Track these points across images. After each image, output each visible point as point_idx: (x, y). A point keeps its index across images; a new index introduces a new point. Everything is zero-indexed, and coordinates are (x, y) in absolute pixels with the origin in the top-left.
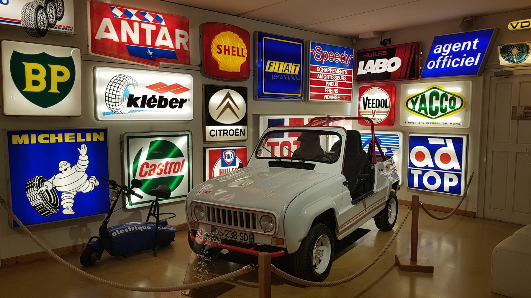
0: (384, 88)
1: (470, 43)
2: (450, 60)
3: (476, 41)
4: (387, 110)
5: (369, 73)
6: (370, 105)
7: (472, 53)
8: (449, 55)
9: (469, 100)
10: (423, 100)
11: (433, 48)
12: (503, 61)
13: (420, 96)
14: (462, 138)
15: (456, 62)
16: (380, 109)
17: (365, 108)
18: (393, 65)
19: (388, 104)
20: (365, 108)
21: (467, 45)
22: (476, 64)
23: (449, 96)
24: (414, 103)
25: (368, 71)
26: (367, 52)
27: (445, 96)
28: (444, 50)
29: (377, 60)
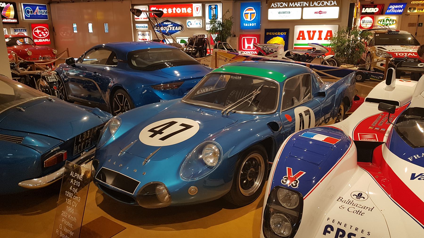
0: (371, 17)
1: (400, 6)
2: (394, 10)
3: (402, 6)
4: (372, 24)
5: (366, 12)
6: (365, 22)
7: (401, 9)
8: (394, 9)
9: (397, 21)
11: (389, 6)
12: (408, 11)
13: (383, 20)
15: (396, 11)
16: (369, 23)
18: (376, 10)
19: (372, 22)
21: (399, 6)
22: (401, 12)
23: (392, 20)
24: (381, 22)
25: (366, 11)
26: (367, 5)
27: (391, 20)
28: (392, 7)
29: (370, 8)
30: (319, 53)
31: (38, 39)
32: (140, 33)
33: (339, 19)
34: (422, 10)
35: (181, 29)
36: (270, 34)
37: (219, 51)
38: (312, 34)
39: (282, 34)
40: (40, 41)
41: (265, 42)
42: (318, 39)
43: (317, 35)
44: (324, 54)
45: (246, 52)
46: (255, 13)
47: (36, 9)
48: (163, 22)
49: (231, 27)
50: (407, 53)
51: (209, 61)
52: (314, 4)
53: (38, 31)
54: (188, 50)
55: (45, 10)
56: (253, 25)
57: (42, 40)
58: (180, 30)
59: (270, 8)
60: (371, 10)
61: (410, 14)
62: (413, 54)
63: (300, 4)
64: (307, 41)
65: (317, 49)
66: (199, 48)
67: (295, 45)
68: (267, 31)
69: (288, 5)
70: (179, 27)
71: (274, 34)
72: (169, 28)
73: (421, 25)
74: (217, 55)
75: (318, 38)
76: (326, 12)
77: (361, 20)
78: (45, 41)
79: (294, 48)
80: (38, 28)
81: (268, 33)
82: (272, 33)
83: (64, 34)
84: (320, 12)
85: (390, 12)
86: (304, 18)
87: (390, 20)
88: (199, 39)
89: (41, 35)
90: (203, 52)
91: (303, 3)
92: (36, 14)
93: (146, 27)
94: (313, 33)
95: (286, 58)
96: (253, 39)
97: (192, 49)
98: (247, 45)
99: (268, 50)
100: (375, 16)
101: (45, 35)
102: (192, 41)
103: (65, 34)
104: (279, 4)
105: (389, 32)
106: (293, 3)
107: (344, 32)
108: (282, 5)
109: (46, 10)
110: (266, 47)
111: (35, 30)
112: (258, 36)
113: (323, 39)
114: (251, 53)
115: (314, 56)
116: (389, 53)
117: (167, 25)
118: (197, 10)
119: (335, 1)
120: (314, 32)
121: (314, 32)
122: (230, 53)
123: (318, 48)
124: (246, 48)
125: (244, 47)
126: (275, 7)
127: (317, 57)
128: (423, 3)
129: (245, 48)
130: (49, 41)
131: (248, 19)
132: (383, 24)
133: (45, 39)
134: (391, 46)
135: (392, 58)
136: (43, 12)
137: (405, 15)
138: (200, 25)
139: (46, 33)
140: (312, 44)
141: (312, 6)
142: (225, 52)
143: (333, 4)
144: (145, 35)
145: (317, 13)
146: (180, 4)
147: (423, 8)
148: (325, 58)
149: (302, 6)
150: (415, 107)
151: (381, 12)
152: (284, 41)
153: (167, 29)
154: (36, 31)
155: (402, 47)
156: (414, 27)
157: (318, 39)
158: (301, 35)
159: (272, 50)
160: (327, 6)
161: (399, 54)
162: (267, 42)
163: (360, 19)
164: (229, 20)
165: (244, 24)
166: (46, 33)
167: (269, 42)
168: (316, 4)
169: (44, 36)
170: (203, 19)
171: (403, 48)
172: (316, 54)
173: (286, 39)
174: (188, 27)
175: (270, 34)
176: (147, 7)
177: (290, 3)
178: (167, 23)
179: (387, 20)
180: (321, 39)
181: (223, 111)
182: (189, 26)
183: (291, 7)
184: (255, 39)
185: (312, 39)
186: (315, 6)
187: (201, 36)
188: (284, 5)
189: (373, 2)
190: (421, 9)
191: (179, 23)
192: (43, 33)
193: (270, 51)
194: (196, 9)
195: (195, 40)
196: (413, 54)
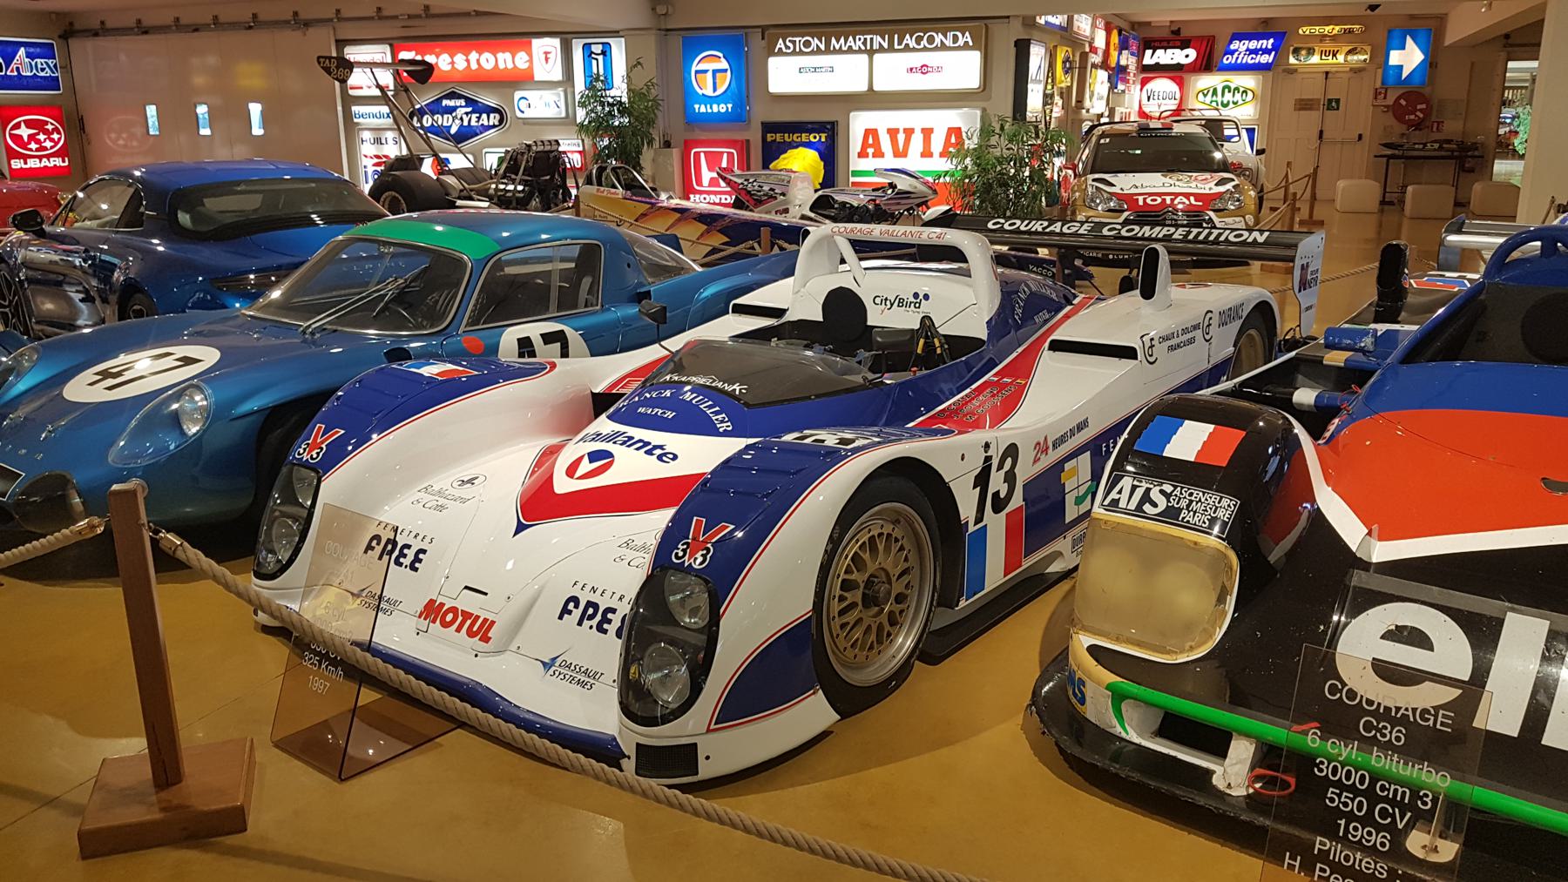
0: (1172, 78)
1: (1265, 41)
3: (1271, 41)
4: (1177, 102)
5: (1157, 64)
6: (1156, 97)
7: (1266, 51)
8: (1246, 51)
9: (1259, 92)
10: (1215, 92)
11: (1231, 43)
12: (1292, 60)
13: (1212, 90)
14: (1254, 129)
15: (1252, 58)
16: (1167, 101)
17: (1149, 100)
18: (1187, 56)
19: (1178, 96)
20: (1149, 100)
22: (1270, 61)
23: (1241, 89)
24: (1205, 95)
26: (1157, 41)
27: (1237, 89)
28: (1240, 46)
29: (1168, 51)
30: (908, 198)
31: (25, 158)
32: (366, 135)
33: (981, 89)
34: (1334, 55)
35: (499, 121)
36: (778, 140)
37: (599, 194)
38: (901, 137)
39: (815, 137)
40: (33, 166)
41: (766, 166)
42: (923, 155)
43: (917, 142)
44: (927, 201)
45: (705, 199)
46: (729, 72)
47: (17, 57)
49: (655, 114)
50: (1173, 197)
52: (905, 42)
53: (24, 132)
54: (502, 190)
55: (49, 59)
56: (723, 108)
57: (40, 162)
58: (494, 126)
59: (772, 53)
60: (1173, 56)
61: (1299, 70)
62: (1192, 198)
63: (863, 43)
64: (889, 161)
65: (899, 187)
66: (539, 183)
67: (855, 173)
68: (768, 127)
69: (828, 44)
70: (492, 115)
72: (459, 117)
73: (1334, 104)
74: (581, 204)
75: (922, 153)
76: (940, 69)
77: (1141, 90)
78: (49, 165)
79: (852, 183)
80: (25, 121)
83: (118, 139)
84: (924, 70)
85: (1233, 62)
87: (1235, 89)
88: (537, 152)
89: (37, 146)
90: (551, 195)
91: (872, 39)
92: (16, 73)
93: (386, 116)
95: (812, 215)
96: (725, 155)
97: (515, 188)
98: (707, 176)
99: (760, 191)
100: (1186, 76)
101: (52, 144)
102: (516, 160)
103: (124, 139)
104: (800, 41)
105: (1141, 129)
106: (842, 40)
107: (993, 131)
108: (807, 44)
109: (55, 61)
110: (755, 181)
111: (12, 129)
112: (744, 147)
114: (721, 199)
115: (893, 208)
116: (1121, 197)
117: (454, 109)
118: (547, 59)
119: (967, 34)
120: (909, 132)
121: (909, 132)
122: (631, 200)
123: (903, 184)
124: (704, 185)
125: (699, 183)
126: (788, 51)
127: (906, 213)
128: (1335, 32)
129: (702, 186)
130: (66, 164)
131: (706, 89)
132: (1214, 104)
133: (52, 159)
134: (1132, 175)
135: (1126, 214)
136: (44, 67)
137: (1284, 71)
139: (52, 136)
140: (886, 170)
141: (900, 47)
142: (617, 196)
143: (961, 42)
144: (384, 141)
145: (914, 70)
146: (492, 41)
147: (1338, 51)
148: (927, 214)
149: (868, 48)
150: (799, 320)
151: (1206, 64)
152: (822, 163)
154: (14, 132)
155: (1165, 176)
156: (1313, 112)
157: (923, 155)
158: (871, 141)
159: (772, 190)
160: (943, 47)
161: (1149, 201)
162: (771, 166)
163: (1139, 87)
164: (643, 91)
165: (697, 106)
166: (56, 136)
168: (912, 44)
169: (45, 149)
170: (569, 90)
171: (1167, 180)
172: (899, 204)
173: (830, 156)
174: (519, 114)
176: (387, 49)
177: (833, 40)
178: (453, 101)
179: (1226, 90)
180: (931, 155)
181: (302, 329)
182: (523, 112)
183: (835, 52)
184: (730, 155)
185: (904, 154)
186: (907, 49)
187: (546, 143)
188: (813, 46)
189: (1179, 29)
190: (1330, 51)
191: (491, 101)
192: (42, 137)
193: (764, 195)
194: (544, 56)
195: (526, 156)
196: (1189, 200)
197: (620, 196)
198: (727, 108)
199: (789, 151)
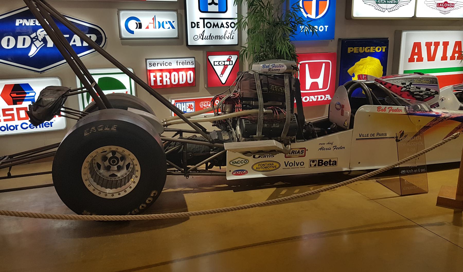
38: (433, 48)
39: (379, 49)
48: (13, 19)
51: (341, 148)
71: (363, 51)
72: (40, 38)
76: (453, 5)
81: (351, 50)
82: (359, 49)
86: (418, 16)
94: (434, 46)
96: (324, 64)
98: (309, 81)
110: (411, 84)
113: (449, 58)
114: (318, 98)
120: (437, 44)
121: (437, 44)
131: (311, 14)
138: (173, 28)
142: (400, 113)
145: (441, 5)
153: (32, 42)
159: (427, 90)
167: (354, 69)
174: (125, 34)
175: (355, 50)
184: (327, 64)
197: (404, 112)
198: (325, 28)
199: (361, 60)
